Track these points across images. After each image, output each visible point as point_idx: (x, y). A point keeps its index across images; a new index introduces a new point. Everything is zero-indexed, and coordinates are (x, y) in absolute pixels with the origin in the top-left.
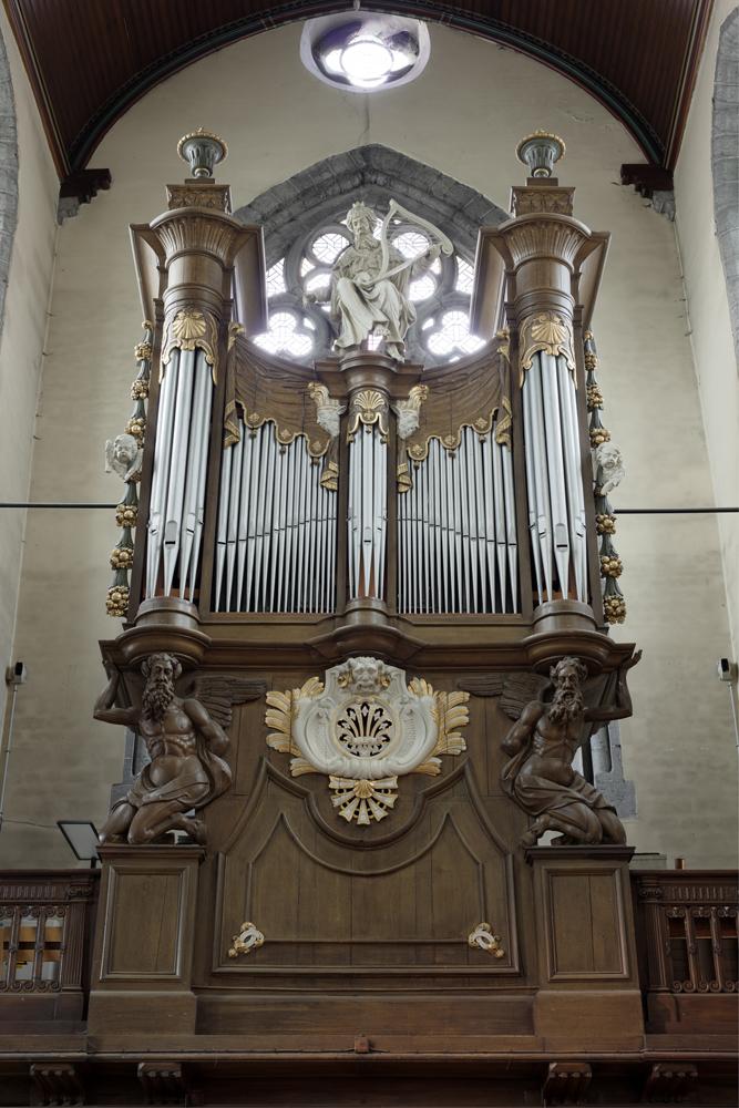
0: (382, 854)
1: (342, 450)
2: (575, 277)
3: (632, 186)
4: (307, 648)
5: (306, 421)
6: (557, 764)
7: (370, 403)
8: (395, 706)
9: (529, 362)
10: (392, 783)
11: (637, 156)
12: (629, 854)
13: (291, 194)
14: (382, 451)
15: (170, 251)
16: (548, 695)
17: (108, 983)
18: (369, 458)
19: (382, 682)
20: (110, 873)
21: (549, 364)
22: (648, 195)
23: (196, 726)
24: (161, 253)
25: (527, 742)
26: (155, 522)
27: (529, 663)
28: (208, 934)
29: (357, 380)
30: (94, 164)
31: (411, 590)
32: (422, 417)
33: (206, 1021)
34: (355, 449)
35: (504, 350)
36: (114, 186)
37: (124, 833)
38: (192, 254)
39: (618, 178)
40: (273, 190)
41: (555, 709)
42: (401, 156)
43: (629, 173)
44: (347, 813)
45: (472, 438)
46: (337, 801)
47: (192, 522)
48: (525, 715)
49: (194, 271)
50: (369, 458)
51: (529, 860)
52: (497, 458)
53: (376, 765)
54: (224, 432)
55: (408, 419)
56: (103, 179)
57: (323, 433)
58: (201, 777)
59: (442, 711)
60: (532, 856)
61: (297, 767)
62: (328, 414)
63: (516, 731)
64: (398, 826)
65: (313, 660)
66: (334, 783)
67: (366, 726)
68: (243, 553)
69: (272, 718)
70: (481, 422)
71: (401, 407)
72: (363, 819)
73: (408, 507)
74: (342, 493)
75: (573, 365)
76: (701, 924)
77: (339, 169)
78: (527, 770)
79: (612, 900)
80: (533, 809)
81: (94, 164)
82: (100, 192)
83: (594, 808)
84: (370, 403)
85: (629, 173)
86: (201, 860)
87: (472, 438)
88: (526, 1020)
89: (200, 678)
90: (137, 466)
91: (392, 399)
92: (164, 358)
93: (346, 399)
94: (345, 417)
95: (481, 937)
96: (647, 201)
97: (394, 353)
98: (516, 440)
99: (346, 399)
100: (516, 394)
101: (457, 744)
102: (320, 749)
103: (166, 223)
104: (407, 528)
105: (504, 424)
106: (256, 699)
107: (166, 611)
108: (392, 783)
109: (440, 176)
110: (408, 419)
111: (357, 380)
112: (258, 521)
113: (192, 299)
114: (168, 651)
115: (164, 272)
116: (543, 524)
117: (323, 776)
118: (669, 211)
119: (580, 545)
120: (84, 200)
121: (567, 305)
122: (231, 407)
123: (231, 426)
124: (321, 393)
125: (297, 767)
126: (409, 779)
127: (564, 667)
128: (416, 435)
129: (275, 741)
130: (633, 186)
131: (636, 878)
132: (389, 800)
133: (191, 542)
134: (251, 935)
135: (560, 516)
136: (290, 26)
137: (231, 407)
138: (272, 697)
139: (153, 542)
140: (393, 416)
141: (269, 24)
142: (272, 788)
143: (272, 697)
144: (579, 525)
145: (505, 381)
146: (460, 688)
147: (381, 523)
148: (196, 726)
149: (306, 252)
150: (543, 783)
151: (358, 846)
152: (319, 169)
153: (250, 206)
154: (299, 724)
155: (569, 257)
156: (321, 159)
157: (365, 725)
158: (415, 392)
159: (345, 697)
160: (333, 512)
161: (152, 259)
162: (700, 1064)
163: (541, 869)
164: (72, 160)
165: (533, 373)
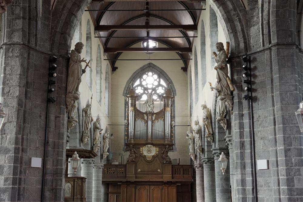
0: (151, 163)
1: (147, 122)
2: (171, 101)
3: (182, 70)
4: (144, 144)
5: (143, 118)
6: (166, 155)
7: (150, 117)
8: (152, 149)
9: (166, 112)
10: (151, 156)
11: (183, 66)
12: (172, 163)
13: (140, 70)
14: (151, 122)
15: (129, 99)
16: (166, 148)
17: (128, 174)
18: (150, 123)
19: (151, 147)
20: (127, 165)
21: (168, 113)
22: (184, 71)
23: (134, 151)
24: (129, 99)
25: (164, 153)
26: (129, 131)
27: (164, 145)
28: (136, 170)
29: (149, 115)
30: (116, 66)
31: (153, 137)
32: (155, 118)
33: (136, 178)
34: (148, 122)
35: (163, 110)
36: (118, 69)
37: (128, 161)
38: (132, 100)
39: (181, 69)
40: (138, 69)
41: (166, 150)
42: (154, 64)
43: (182, 68)
44: (148, 159)
45: (160, 120)
46: (147, 158)
47: (133, 131)
48: (164, 150)
49: (132, 101)
50: (150, 123)
51: (163, 164)
52: (162, 122)
53: (150, 155)
54: (135, 120)
55: (154, 118)
56: (117, 68)
57: (145, 120)
58: (135, 156)
59: (156, 150)
60: (164, 163)
61: (143, 155)
62: (146, 118)
63: (163, 152)
64: (152, 161)
65: (145, 145)
66: (146, 156)
67: (149, 151)
68: (138, 133)
69: (141, 150)
70: (161, 118)
71: (153, 117)
72: (149, 160)
73: (153, 128)
74: (147, 125)
75: (170, 112)
76: (178, 169)
77: (146, 66)
78: (164, 155)
79: (170, 168)
80: (164, 159)
81: (116, 66)
82: (117, 70)
83: (169, 159)
84: (150, 117)
85: (182, 68)
86: (135, 164)
87: (160, 120)
88: (162, 178)
89: (134, 146)
90: (127, 124)
91: (152, 116)
92: (129, 112)
93: (148, 116)
94: (148, 118)
95: (159, 170)
96: (184, 72)
97: (152, 112)
98: (164, 120)
99: (148, 116)
100: (164, 115)
101: (157, 153)
102: (145, 153)
103: (129, 96)
104: (153, 130)
105: (163, 119)
106: (139, 148)
107: (131, 141)
108: (151, 156)
109: (159, 68)
110: (154, 118)
111: (149, 115)
112: (139, 129)
113: (132, 106)
114: (131, 145)
115: (129, 100)
116: (166, 131)
117: (146, 156)
118: (187, 74)
119: (170, 133)
120: (115, 71)
121: (170, 105)
122: (136, 117)
123: (136, 119)
124: (145, 115)
125: (143, 155)
126: (153, 156)
127: (167, 146)
128: (154, 120)
129: (141, 152)
130: (182, 70)
131: (172, 165)
132: (151, 158)
133: (133, 133)
134: (139, 170)
135: (168, 130)
136: (140, 42)
137: (136, 117)
138: (141, 148)
139: (129, 133)
140: (152, 118)
141: (137, 43)
142: (141, 157)
143: (141, 148)
144: (170, 131)
145: (163, 114)
146: (158, 147)
147: (151, 131)
148: (134, 151)
149: (142, 78)
150: (165, 157)
151: (149, 162)
152: (144, 66)
153: (135, 72)
154: (143, 151)
155: (170, 100)
156: (144, 65)
157: (149, 151)
158: (154, 115)
159: (147, 148)
160: (146, 129)
161: (127, 99)
162: (176, 181)
163: (164, 165)
164: (113, 65)
165: (166, 113)
